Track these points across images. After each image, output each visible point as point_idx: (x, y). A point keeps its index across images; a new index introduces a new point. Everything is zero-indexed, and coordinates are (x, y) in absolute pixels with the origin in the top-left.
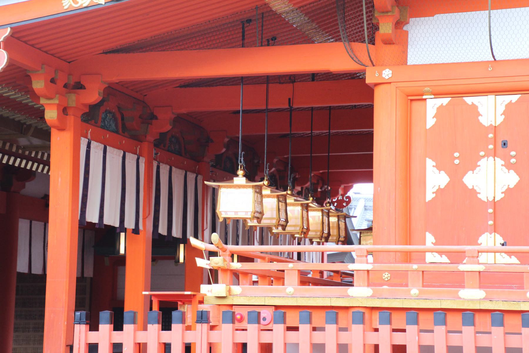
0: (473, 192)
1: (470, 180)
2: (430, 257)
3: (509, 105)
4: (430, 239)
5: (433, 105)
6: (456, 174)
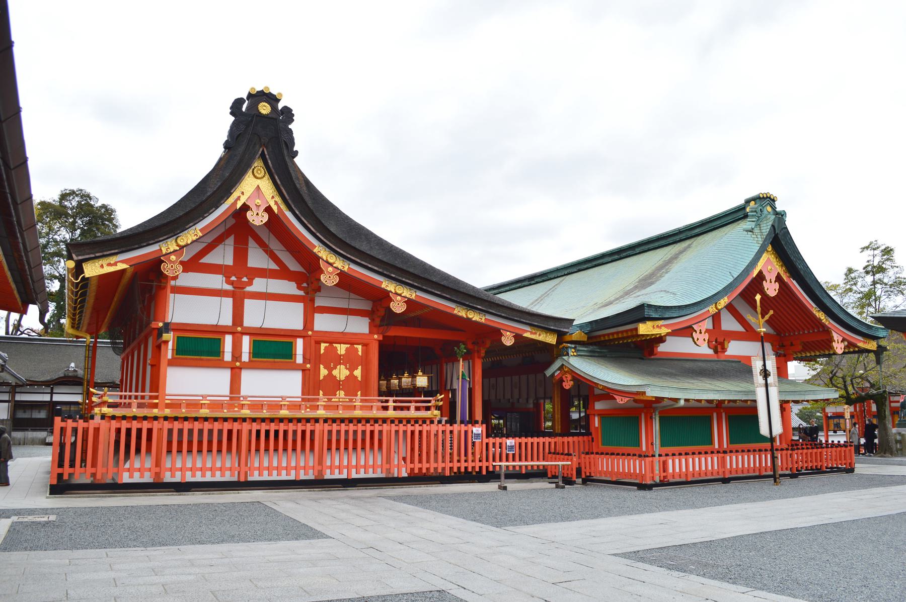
1: (335, 373)
3: (347, 349)
4: (321, 392)
5: (323, 346)
6: (330, 370)
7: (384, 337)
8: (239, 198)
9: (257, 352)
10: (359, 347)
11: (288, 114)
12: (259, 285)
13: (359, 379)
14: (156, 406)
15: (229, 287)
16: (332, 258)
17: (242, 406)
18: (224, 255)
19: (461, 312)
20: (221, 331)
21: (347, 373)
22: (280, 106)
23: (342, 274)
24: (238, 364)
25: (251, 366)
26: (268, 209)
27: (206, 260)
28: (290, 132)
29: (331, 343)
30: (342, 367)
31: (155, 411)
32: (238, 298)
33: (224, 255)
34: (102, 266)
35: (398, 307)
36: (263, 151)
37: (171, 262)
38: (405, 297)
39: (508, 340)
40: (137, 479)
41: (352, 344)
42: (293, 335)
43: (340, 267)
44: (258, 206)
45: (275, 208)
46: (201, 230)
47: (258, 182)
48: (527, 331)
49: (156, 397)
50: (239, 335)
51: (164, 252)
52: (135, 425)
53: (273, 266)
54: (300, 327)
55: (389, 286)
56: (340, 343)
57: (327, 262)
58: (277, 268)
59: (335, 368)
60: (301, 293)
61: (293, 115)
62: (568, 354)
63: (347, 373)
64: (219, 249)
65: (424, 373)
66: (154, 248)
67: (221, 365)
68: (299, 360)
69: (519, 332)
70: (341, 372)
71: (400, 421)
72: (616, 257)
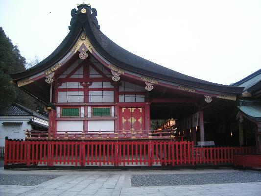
5: (123, 109)
6: (127, 119)
9: (93, 113)
10: (141, 109)
11: (94, 11)
12: (95, 85)
14: (47, 136)
15: (82, 87)
18: (80, 74)
23: (121, 76)
26: (88, 52)
27: (73, 77)
30: (133, 118)
31: (47, 138)
32: (86, 90)
33: (80, 74)
39: (208, 100)
40: (43, 164)
45: (91, 51)
48: (218, 95)
52: (37, 143)
54: (112, 101)
58: (101, 77)
59: (129, 118)
64: (77, 73)
66: (43, 73)
69: (215, 96)
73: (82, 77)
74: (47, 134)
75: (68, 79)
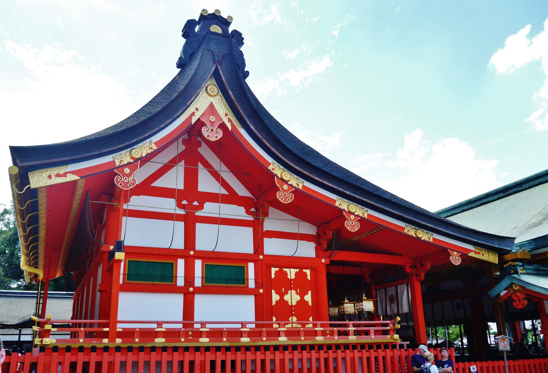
0: (287, 302)
1: (287, 298)
2: (275, 326)
3: (296, 273)
4: (274, 319)
5: (274, 270)
6: (282, 295)
7: (331, 261)
8: (193, 114)
11: (238, 38)
12: (210, 209)
13: (310, 304)
14: (106, 335)
15: (182, 212)
16: (287, 175)
17: (200, 334)
19: (410, 231)
20: (174, 254)
21: (298, 298)
22: (231, 29)
24: (191, 289)
25: (204, 290)
26: (222, 126)
27: (159, 183)
28: (241, 54)
29: (281, 267)
30: (293, 291)
31: (106, 341)
32: (190, 222)
34: (50, 177)
35: (352, 226)
36: (217, 66)
37: (125, 175)
38: (358, 216)
41: (301, 268)
42: (244, 258)
43: (295, 185)
44: (212, 123)
46: (155, 143)
47: (212, 99)
49: (107, 325)
50: (191, 259)
51: (117, 163)
53: (224, 192)
55: (342, 204)
56: (290, 268)
57: (282, 179)
58: (227, 193)
59: (287, 293)
60: (250, 218)
61: (243, 39)
62: (516, 272)
63: (298, 298)
65: (350, 301)
66: (108, 159)
67: (174, 289)
68: (252, 284)
70: (292, 298)
71: (362, 346)
72: (502, 195)
73: (181, 186)
74: (107, 329)
75: (146, 188)
